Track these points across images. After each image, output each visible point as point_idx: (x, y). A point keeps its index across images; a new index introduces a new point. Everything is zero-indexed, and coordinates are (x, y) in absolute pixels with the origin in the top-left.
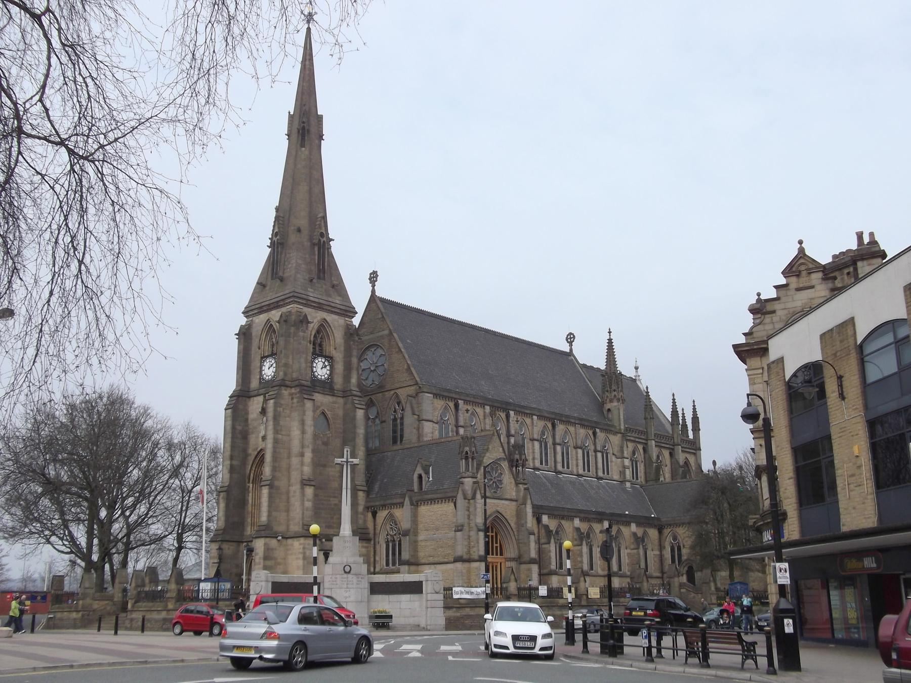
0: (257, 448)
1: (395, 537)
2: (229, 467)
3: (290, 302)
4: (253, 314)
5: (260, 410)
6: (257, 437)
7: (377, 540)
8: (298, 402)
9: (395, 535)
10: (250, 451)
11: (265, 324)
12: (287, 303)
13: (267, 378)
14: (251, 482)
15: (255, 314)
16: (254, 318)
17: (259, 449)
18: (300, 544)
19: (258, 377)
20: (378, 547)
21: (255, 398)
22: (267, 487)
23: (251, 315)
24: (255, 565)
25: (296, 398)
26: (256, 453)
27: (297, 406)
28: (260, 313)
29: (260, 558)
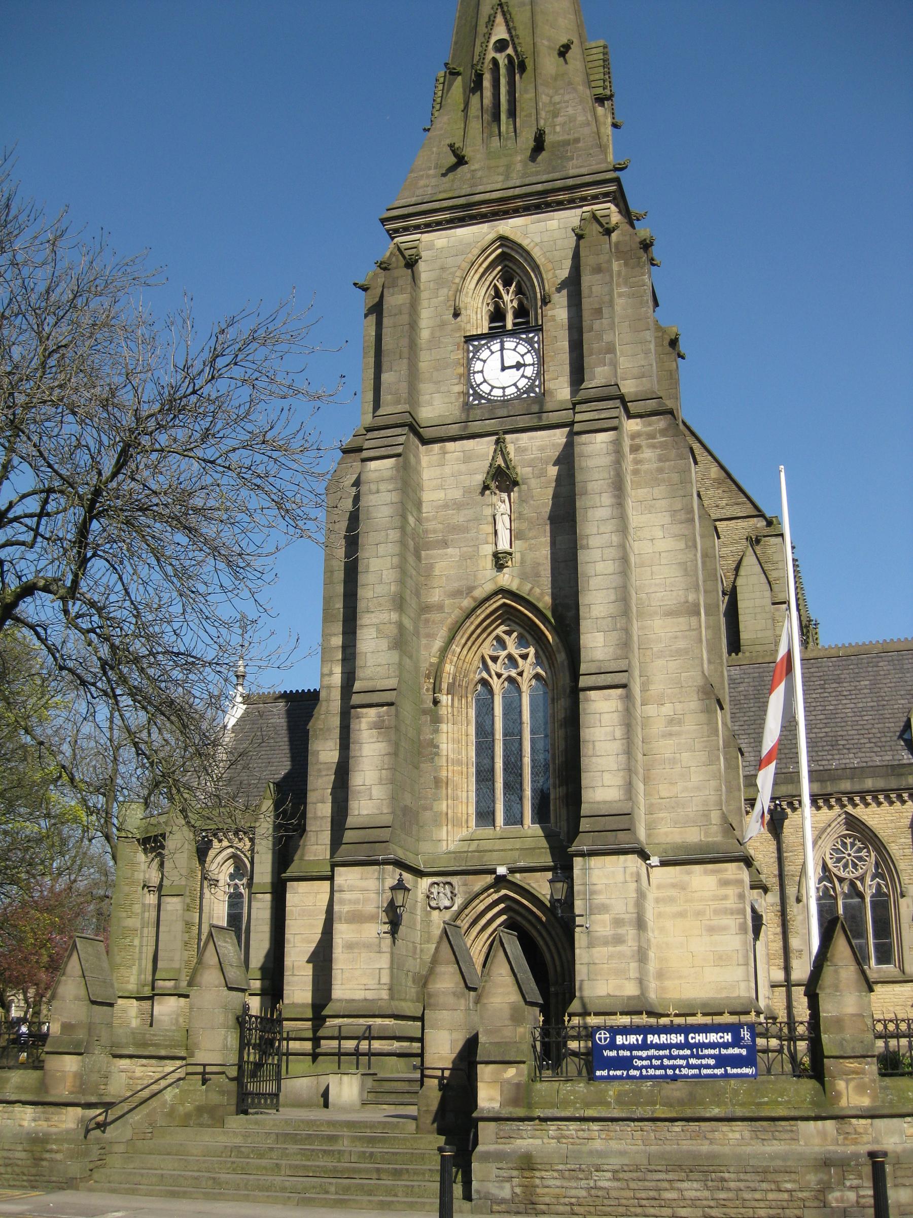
0: (470, 589)
1: (858, 883)
2: (392, 630)
3: (595, 197)
4: (428, 225)
5: (480, 478)
6: (473, 556)
7: (791, 891)
8: (661, 459)
9: (862, 879)
10: (435, 596)
11: (484, 251)
12: (584, 199)
13: (497, 393)
14: (444, 686)
15: (439, 223)
16: (426, 237)
17: (480, 593)
18: (725, 883)
19: (458, 388)
20: (794, 909)
21: (450, 446)
22: (619, 691)
23: (417, 227)
24: (590, 945)
25: (653, 446)
26: (467, 603)
27: (660, 470)
28: (461, 222)
29: (618, 922)
